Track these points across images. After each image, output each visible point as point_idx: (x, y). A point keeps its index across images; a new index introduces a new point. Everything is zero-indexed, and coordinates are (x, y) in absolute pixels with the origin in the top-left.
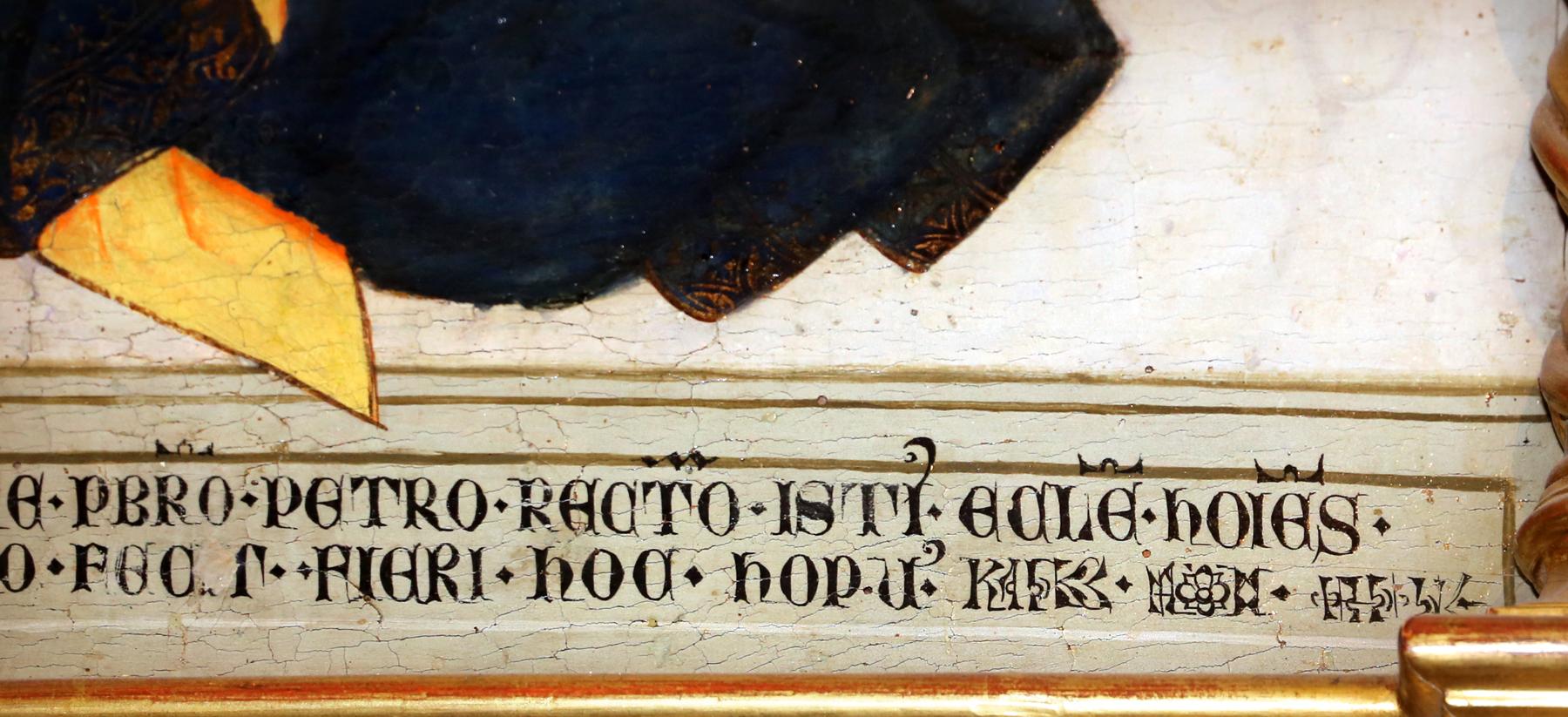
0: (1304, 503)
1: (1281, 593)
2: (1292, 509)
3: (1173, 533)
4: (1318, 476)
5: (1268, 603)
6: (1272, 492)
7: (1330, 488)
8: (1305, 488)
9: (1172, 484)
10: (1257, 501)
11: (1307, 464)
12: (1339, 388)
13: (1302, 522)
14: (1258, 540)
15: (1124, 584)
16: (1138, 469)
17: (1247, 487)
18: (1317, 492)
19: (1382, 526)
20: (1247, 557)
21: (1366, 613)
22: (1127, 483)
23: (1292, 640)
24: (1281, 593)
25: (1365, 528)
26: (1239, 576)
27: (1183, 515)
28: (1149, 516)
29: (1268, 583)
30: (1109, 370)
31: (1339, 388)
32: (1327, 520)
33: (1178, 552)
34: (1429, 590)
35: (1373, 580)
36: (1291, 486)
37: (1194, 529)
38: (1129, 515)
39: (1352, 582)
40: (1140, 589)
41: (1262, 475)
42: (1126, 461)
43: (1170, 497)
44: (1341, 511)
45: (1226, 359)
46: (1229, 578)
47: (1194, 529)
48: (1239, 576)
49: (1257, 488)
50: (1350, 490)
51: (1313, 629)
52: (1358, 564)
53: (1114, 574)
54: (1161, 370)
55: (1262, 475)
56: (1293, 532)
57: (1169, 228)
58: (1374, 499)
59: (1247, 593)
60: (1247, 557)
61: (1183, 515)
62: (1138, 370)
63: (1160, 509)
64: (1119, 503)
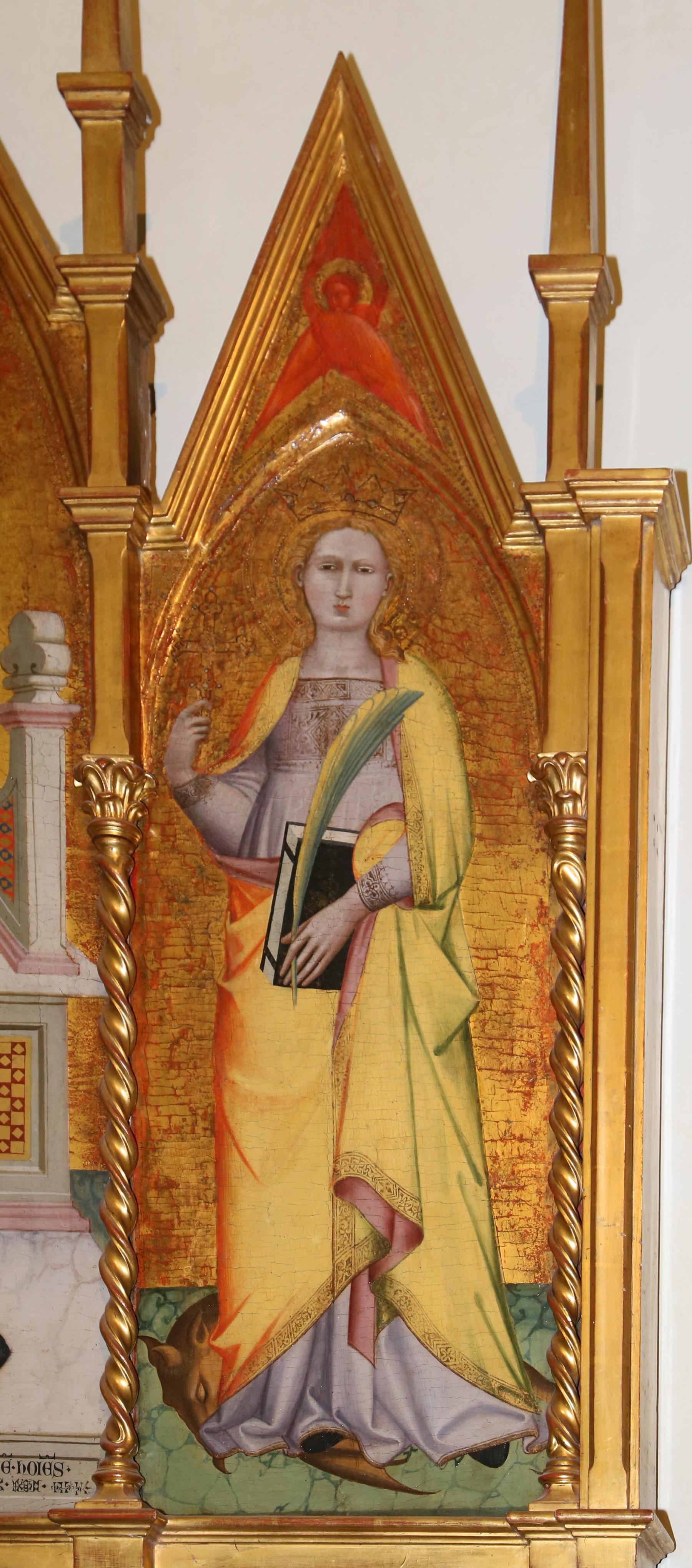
0: (50, 1464)
1: (44, 1486)
2: (47, 1466)
3: (19, 1472)
4: (54, 1458)
5: (41, 1489)
6: (43, 1461)
7: (57, 1460)
8: (51, 1461)
9: (19, 1460)
10: (39, 1464)
11: (51, 1455)
12: (60, 1436)
13: (50, 1469)
14: (39, 1474)
15: (7, 1484)
16: (11, 1456)
17: (37, 1460)
18: (53, 1461)
19: (69, 1470)
20: (36, 1478)
21: (64, 1491)
22: (8, 1459)
23: (47, 1498)
24: (44, 1486)
25: (65, 1470)
26: (34, 1482)
27: (21, 1467)
28: (13, 1468)
29: (41, 1484)
30: (5, 1431)
31: (60, 1436)
32: (56, 1469)
33: (20, 1476)
34: (79, 1485)
35: (66, 1483)
36: (47, 1460)
37: (24, 1471)
38: (9, 1467)
39: (61, 1483)
40: (11, 1486)
41: (41, 1457)
42: (8, 1454)
43: (19, 1463)
44: (59, 1466)
45: (33, 1429)
46: (32, 1482)
47: (24, 1471)
48: (34, 1482)
49: (39, 1460)
50: (61, 1461)
51: (51, 1495)
52: (63, 1479)
53: (5, 1482)
54: (18, 1431)
55: (41, 1457)
56: (48, 1471)
57: (21, 1396)
58: (67, 1463)
59: (36, 1486)
60: (36, 1478)
61: (21, 1467)
62: (12, 1431)
63: (16, 1466)
64: (6, 1464)
